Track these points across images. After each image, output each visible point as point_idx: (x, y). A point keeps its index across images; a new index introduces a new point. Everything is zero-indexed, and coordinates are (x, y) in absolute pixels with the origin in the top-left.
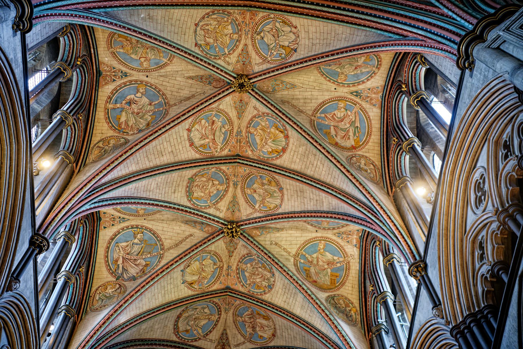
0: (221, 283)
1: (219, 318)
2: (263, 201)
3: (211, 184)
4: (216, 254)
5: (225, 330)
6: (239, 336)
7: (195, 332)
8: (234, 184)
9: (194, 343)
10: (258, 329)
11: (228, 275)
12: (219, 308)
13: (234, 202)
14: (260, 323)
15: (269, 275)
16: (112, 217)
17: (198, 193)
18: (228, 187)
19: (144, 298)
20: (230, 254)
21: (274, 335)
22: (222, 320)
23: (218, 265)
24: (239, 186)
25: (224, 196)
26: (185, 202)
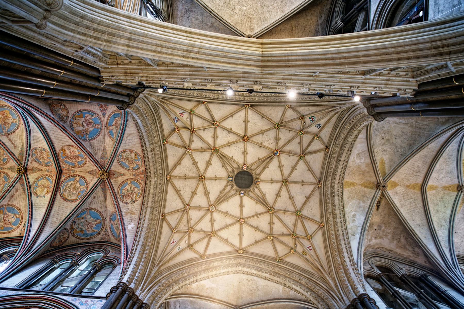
0: (54, 175)
1: (79, 175)
4: (37, 179)
5: (88, 172)
6: (87, 164)
7: (82, 190)
9: (88, 190)
11: (51, 171)
12: (71, 176)
13: (11, 169)
14: (71, 154)
15: (38, 151)
16: (23, 230)
18: (3, 172)
19: (36, 219)
20: (40, 170)
21: (72, 146)
23: (44, 177)
25: (7, 174)
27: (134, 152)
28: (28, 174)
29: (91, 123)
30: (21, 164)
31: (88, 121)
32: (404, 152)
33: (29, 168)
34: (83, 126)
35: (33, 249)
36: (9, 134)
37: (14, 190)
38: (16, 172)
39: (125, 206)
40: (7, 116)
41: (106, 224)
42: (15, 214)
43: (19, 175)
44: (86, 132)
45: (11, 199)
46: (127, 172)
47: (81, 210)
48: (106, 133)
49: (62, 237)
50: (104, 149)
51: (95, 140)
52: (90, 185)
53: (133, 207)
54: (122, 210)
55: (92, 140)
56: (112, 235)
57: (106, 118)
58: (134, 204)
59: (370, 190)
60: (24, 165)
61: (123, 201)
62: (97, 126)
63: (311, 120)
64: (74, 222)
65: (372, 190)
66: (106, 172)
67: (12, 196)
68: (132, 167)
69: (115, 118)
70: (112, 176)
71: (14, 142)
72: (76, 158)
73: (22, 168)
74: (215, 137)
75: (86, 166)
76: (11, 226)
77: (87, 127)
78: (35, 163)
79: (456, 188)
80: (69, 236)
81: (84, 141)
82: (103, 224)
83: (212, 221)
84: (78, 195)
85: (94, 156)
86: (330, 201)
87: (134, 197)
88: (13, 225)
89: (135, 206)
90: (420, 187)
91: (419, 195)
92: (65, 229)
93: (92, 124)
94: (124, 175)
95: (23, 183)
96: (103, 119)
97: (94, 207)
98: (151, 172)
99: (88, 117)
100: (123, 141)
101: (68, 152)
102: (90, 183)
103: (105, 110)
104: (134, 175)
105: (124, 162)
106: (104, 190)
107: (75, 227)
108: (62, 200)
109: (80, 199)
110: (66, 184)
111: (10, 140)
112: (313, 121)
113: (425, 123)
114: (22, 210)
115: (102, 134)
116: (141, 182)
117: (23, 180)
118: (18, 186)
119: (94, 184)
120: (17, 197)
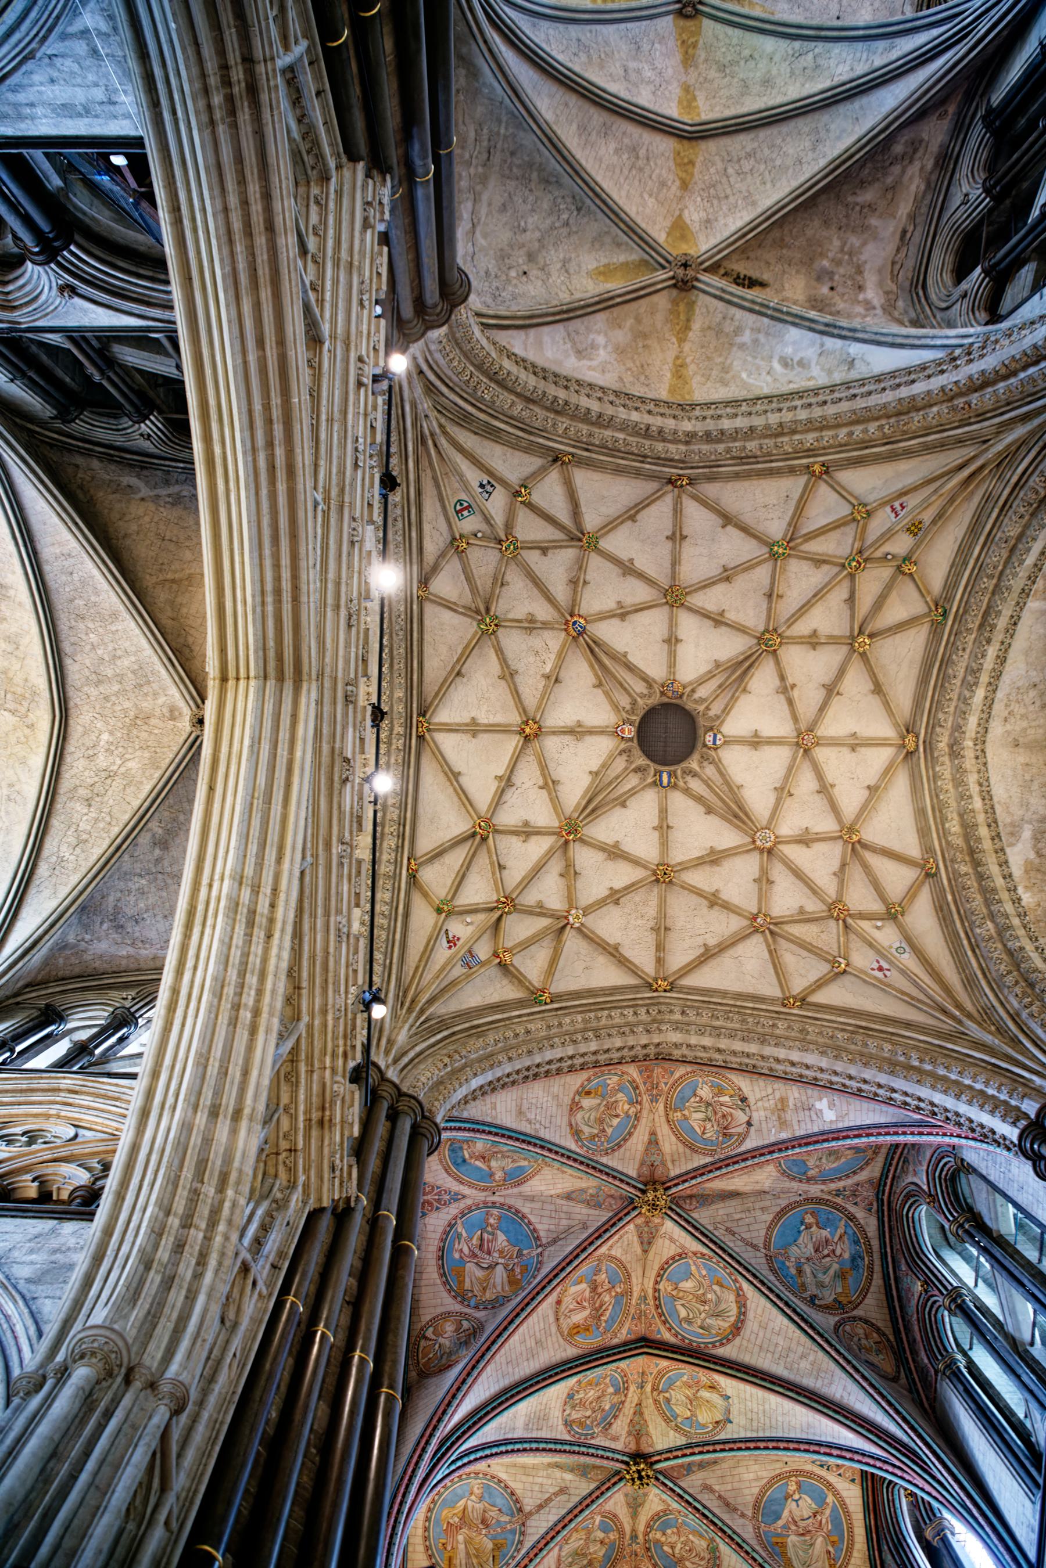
1: (657, 1283)
2: (589, 1532)
3: (677, 1551)
4: (667, 1420)
5: (646, 1251)
6: (619, 1256)
7: (704, 1273)
8: (636, 1537)
9: (705, 1251)
10: (587, 1294)
12: (658, 1307)
13: (635, 1506)
14: (584, 1308)
15: (575, 1415)
16: (841, 1471)
17: (701, 1544)
18: (646, 1534)
20: (639, 1411)
21: (559, 1302)
22: (652, 1274)
24: (628, 1537)
26: (724, 1549)
27: (577, 1098)
28: (651, 1450)
29: (481, 1239)
30: (618, 1473)
31: (477, 1251)
32: (569, 200)
33: (632, 1447)
34: (492, 1267)
35: (905, 1439)
36: (520, 1510)
37: (706, 1498)
38: (646, 1489)
39: (759, 1131)
40: (460, 1515)
41: (819, 1194)
42: (788, 1497)
43: (657, 1479)
44: (511, 1258)
45: (735, 1510)
46: (643, 1121)
47: (772, 1278)
48: (515, 1190)
49: (864, 1341)
50: (568, 1197)
51: (538, 1227)
52: (687, 1245)
53: (760, 1104)
54: (773, 1139)
55: (538, 1238)
56: (855, 1173)
57: (466, 1190)
58: (752, 1100)
59: (697, 311)
60: (623, 1462)
61: (743, 1137)
62: (492, 1221)
63: (465, 513)
64: (812, 1301)
65: (699, 303)
66: (644, 1192)
67: (728, 1505)
68: (626, 1107)
69: (464, 1161)
70: (659, 1172)
71: (547, 1496)
72: (600, 1290)
73: (634, 1468)
74: (527, 832)
75: (623, 1258)
76: (828, 1512)
77: (496, 1255)
78: (614, 1426)
79: (689, 23)
80: (860, 1319)
81: (541, 1262)
82: (820, 1204)
83: (805, 839)
84: (722, 1286)
85: (591, 1230)
86: (737, 444)
87: (725, 1099)
88: (822, 1502)
89: (758, 1096)
90: (685, 142)
91: (711, 146)
92: (836, 1329)
93: (486, 1236)
94: (653, 1133)
95: (682, 1466)
96: (469, 1202)
97: (763, 1232)
98: (644, 1042)
99: (461, 1251)
100: (542, 1134)
101: (578, 1318)
102: (682, 1247)
103: (439, 1194)
104: (654, 1099)
105: (609, 1131)
106: (705, 1199)
107: (828, 1297)
108: (738, 1340)
109: (736, 1281)
110: (685, 1326)
111: (540, 1507)
112: (470, 506)
113: (472, 134)
114: (773, 1474)
115: (518, 1204)
116: (677, 1075)
117: (672, 1468)
118: (692, 1483)
119: (684, 1234)
120: (729, 1487)
